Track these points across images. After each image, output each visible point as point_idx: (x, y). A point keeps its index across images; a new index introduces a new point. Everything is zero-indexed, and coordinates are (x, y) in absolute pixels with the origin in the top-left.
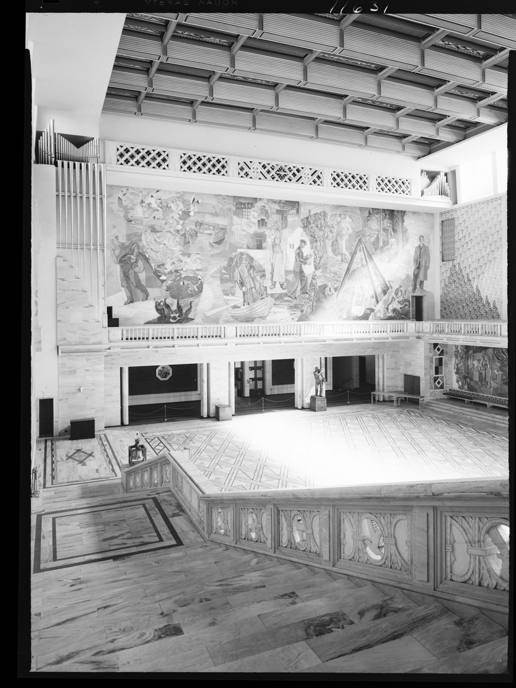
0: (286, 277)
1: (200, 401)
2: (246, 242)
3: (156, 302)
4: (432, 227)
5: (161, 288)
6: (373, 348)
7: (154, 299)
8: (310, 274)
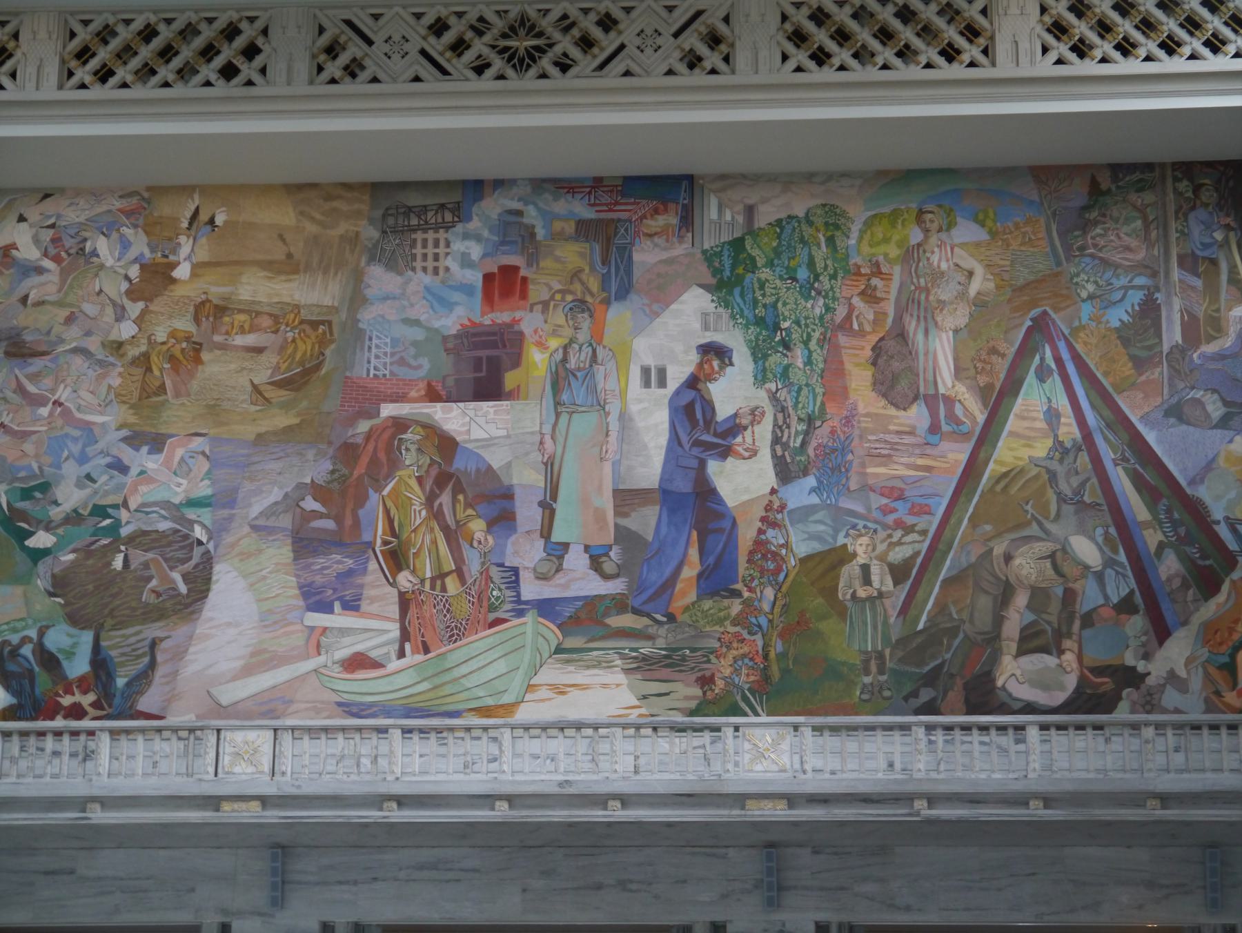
0: (624, 522)
2: (422, 373)
5: (28, 583)
8: (744, 504)
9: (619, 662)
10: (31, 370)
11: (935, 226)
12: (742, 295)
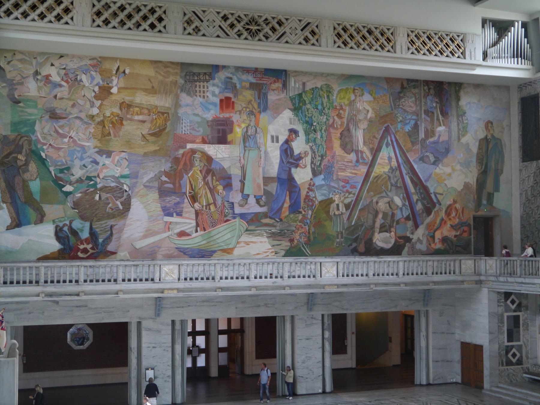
0: (266, 188)
1: (127, 383)
2: (200, 133)
3: (57, 227)
4: (508, 108)
6: (410, 300)
7: (54, 221)
8: (303, 183)
9: (265, 234)
10: (60, 124)
11: (358, 94)
12: (302, 113)
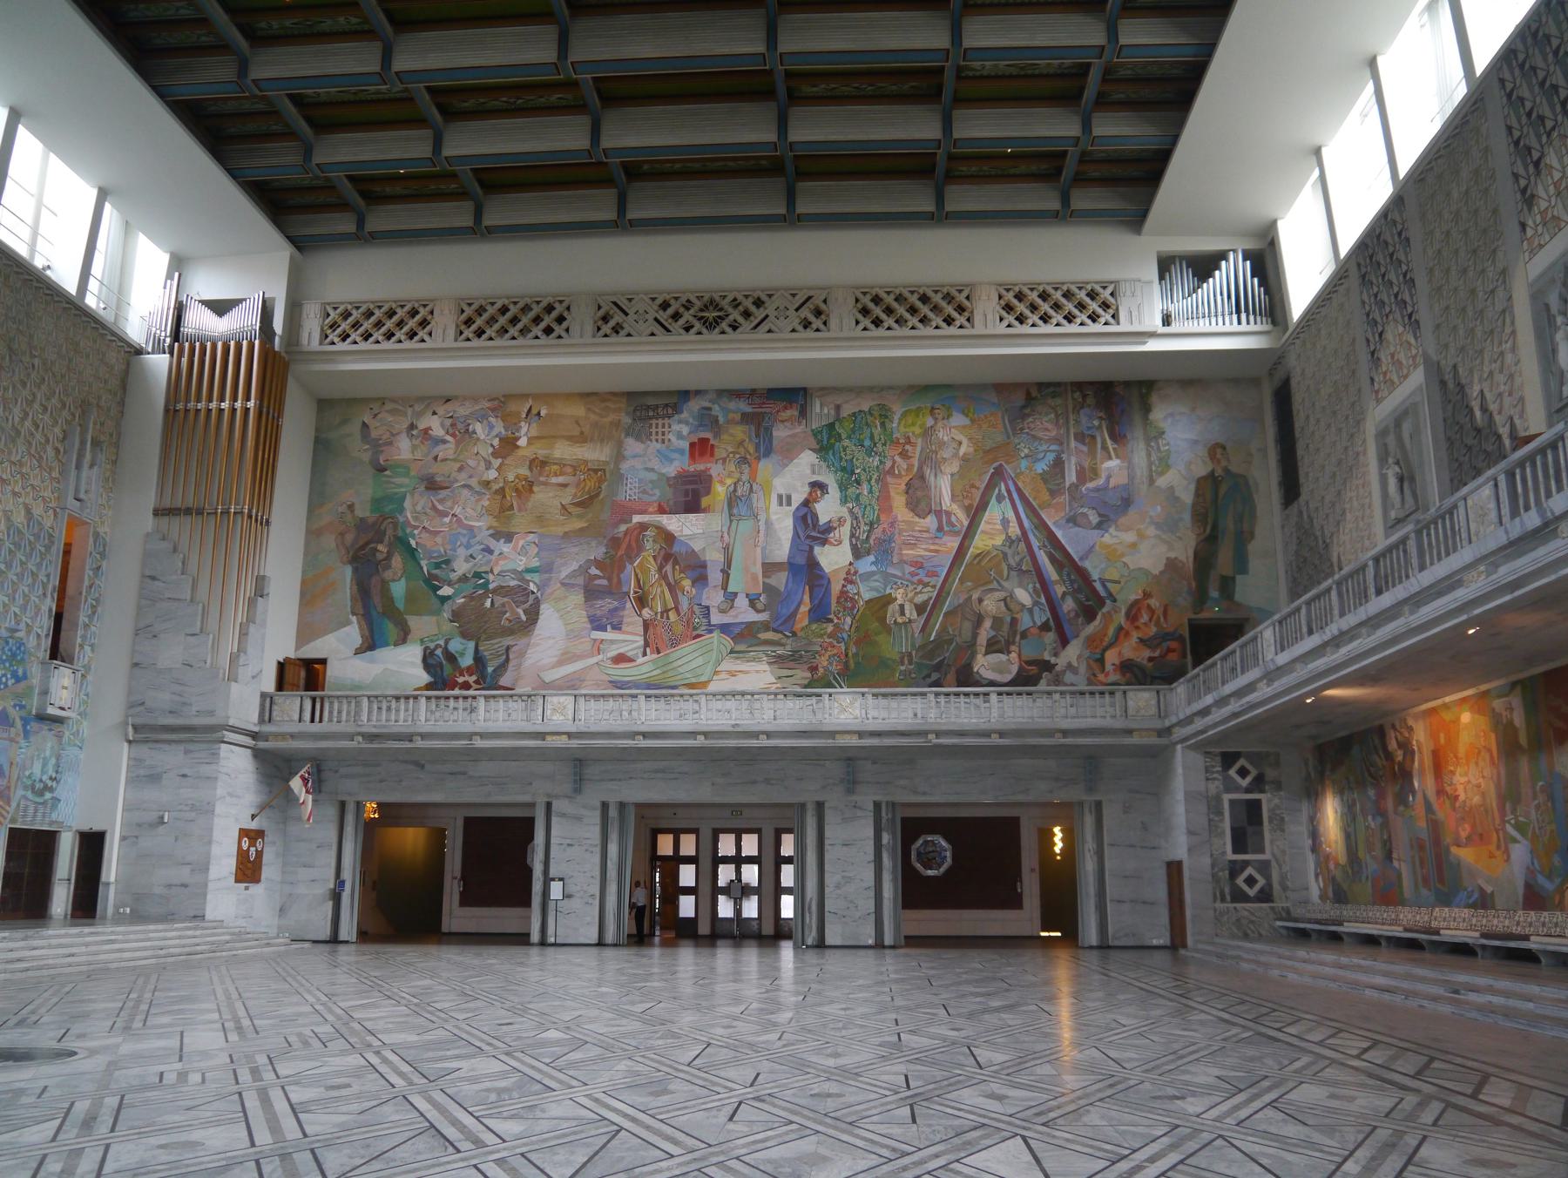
7: (422, 641)
